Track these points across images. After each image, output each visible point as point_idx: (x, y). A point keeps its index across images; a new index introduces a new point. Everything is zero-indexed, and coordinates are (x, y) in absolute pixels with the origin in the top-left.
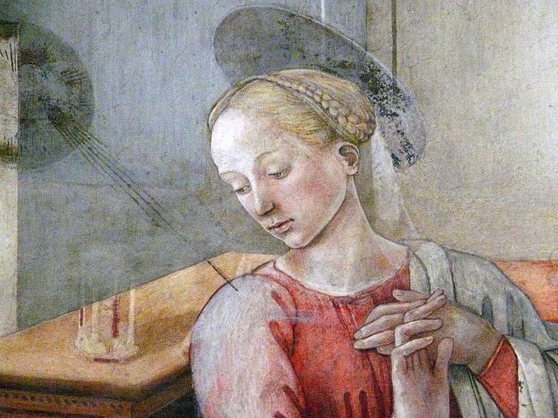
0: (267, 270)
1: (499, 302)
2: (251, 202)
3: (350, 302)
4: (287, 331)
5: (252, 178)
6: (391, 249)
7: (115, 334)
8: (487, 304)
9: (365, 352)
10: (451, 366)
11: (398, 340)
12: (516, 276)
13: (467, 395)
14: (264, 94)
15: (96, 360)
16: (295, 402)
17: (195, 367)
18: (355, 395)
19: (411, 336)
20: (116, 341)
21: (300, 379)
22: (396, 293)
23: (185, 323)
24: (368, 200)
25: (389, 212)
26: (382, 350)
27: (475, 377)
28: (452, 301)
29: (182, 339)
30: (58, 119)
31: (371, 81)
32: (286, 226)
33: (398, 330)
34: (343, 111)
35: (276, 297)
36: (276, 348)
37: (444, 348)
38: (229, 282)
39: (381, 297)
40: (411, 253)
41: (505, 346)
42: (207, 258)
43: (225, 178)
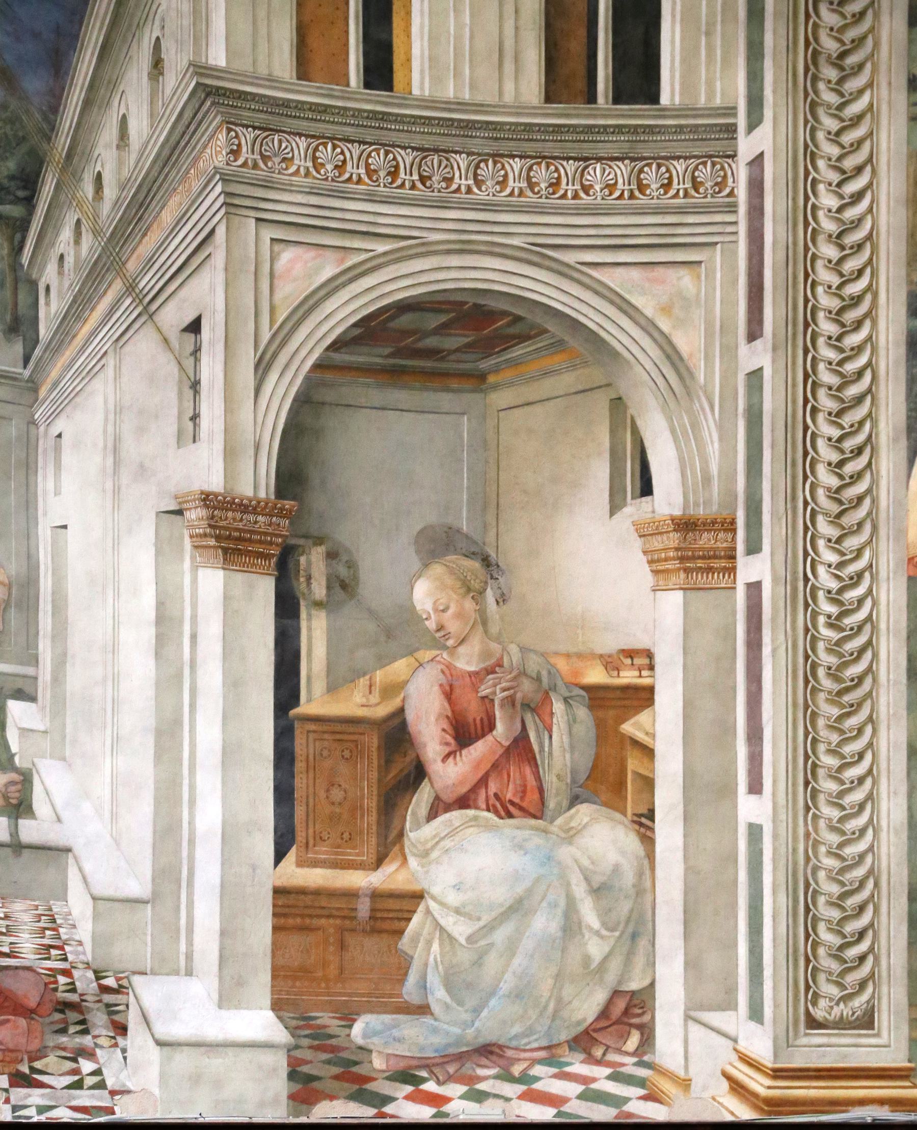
0: (438, 659)
1: (544, 673)
2: (431, 625)
3: (476, 673)
4: (448, 688)
5: (431, 612)
6: (495, 647)
7: (370, 693)
8: (539, 673)
9: (483, 698)
10: (523, 705)
11: (498, 691)
12: (553, 660)
13: (529, 718)
14: (437, 569)
15: (363, 706)
16: (452, 724)
17: (406, 707)
18: (478, 719)
19: (504, 690)
20: (371, 696)
21: (453, 711)
22: (497, 669)
23: (401, 686)
24: (484, 623)
25: (494, 630)
26: (491, 697)
27: (534, 710)
28: (523, 673)
29: (400, 693)
30: (344, 586)
31: (486, 561)
32: (447, 636)
33: (498, 687)
34: (473, 577)
35: (443, 672)
36: (442, 696)
37: (519, 696)
38: (421, 665)
39: (490, 671)
40: (504, 649)
41: (547, 693)
42: (411, 653)
43: (420, 612)
